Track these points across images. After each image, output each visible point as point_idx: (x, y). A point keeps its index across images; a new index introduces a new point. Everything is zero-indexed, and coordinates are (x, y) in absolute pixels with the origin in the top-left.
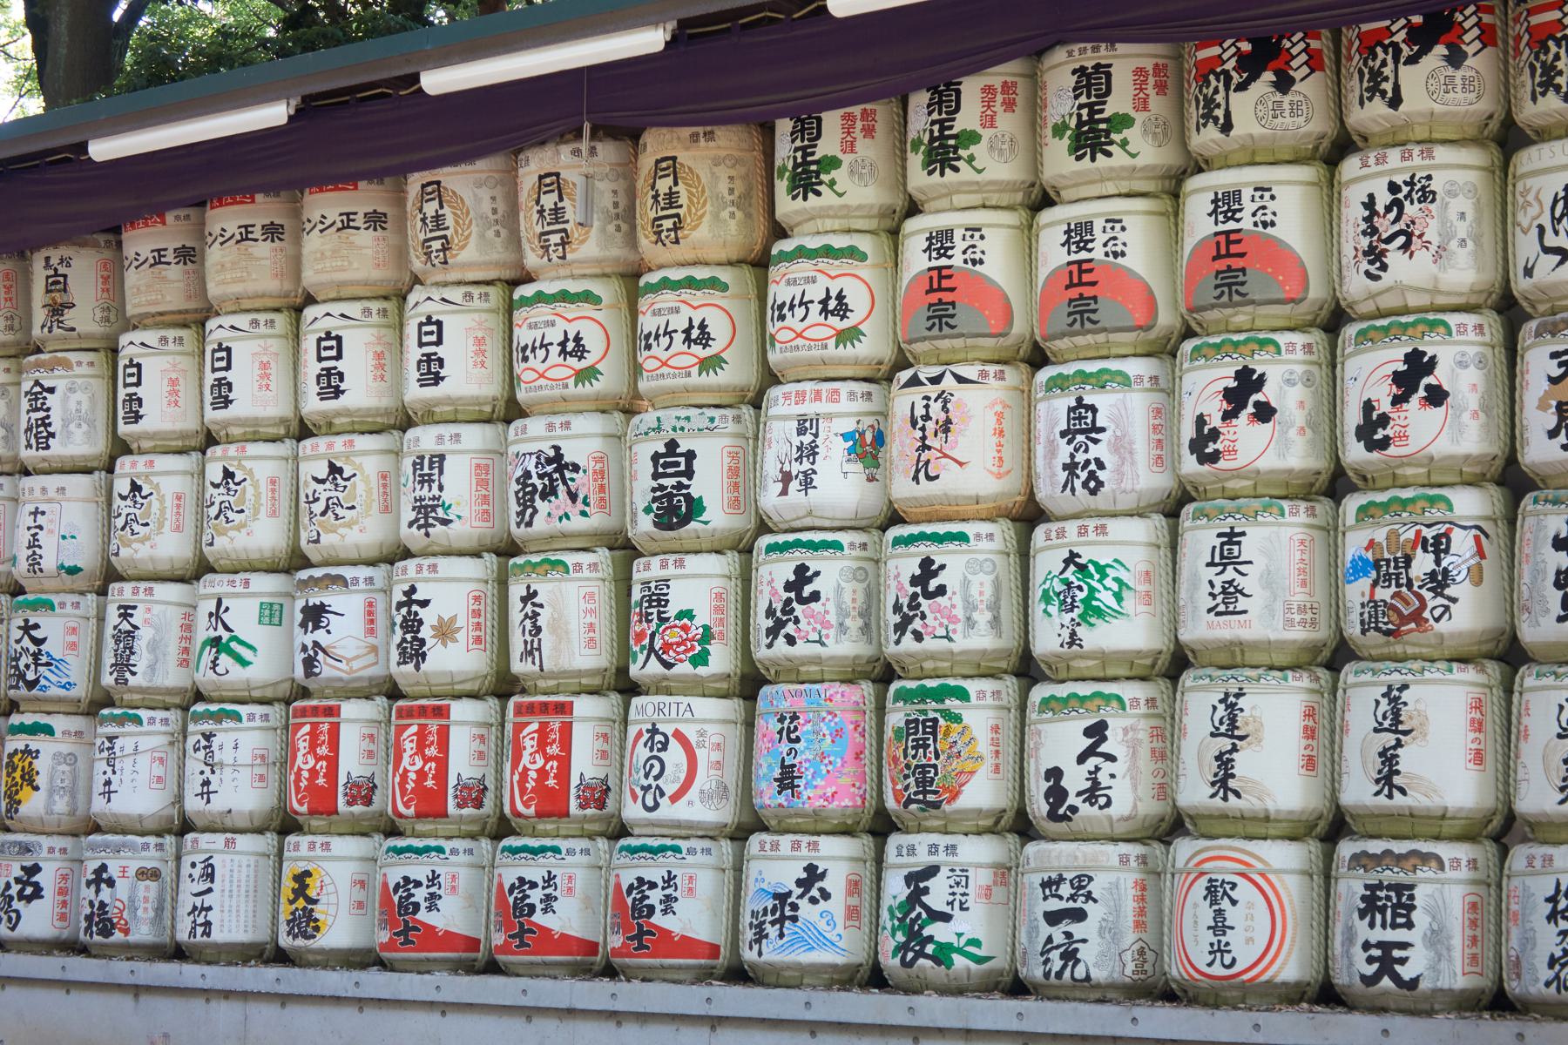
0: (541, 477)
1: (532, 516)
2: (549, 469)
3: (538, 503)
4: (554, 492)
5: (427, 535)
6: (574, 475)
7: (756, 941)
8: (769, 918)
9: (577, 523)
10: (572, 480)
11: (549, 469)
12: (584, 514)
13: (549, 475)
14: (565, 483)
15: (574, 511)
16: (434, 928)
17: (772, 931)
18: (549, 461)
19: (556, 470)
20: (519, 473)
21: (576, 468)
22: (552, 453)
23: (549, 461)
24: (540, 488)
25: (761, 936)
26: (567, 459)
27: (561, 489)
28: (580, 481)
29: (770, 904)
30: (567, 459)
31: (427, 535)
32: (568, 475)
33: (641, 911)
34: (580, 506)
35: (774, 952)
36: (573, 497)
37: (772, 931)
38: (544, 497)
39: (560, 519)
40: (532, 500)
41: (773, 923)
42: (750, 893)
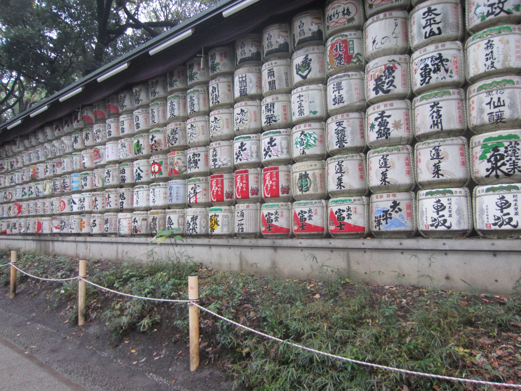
0: (433, 65)
1: (429, 80)
2: (437, 62)
3: (432, 74)
4: (439, 70)
5: (270, 125)
6: (447, 63)
7: (378, 226)
8: (382, 218)
9: (448, 80)
10: (446, 65)
11: (437, 62)
12: (451, 76)
13: (437, 64)
14: (443, 66)
15: (447, 76)
16: (311, 225)
17: (383, 222)
18: (436, 59)
19: (439, 62)
20: (422, 66)
21: (447, 60)
22: (438, 56)
23: (436, 59)
24: (433, 69)
25: (379, 224)
26: (444, 57)
27: (442, 69)
28: (449, 65)
29: (382, 214)
30: (444, 57)
31: (270, 125)
32: (444, 63)
33: (340, 219)
34: (449, 74)
35: (383, 227)
36: (447, 71)
37: (383, 222)
38: (435, 72)
39: (442, 79)
40: (429, 74)
41: (383, 220)
42: (374, 212)
